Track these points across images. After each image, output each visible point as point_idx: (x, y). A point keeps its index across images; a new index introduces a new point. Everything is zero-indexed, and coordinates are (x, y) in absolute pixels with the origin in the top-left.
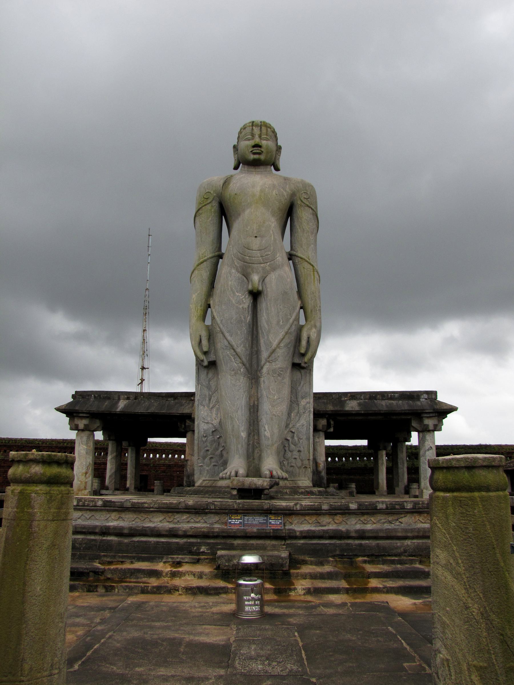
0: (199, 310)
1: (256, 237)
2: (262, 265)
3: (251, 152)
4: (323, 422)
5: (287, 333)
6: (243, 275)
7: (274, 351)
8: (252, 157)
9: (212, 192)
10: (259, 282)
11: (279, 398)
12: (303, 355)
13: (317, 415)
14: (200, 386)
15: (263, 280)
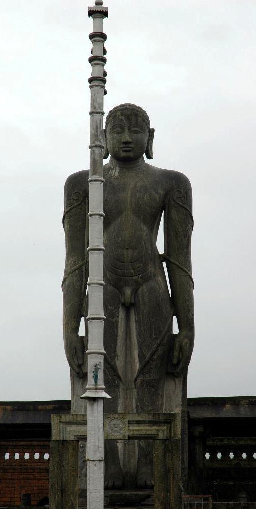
0: (73, 322)
1: (127, 249)
2: (134, 278)
3: (121, 148)
4: (199, 430)
5: (159, 345)
6: (115, 287)
7: (147, 362)
8: (123, 154)
9: (81, 193)
10: (132, 294)
11: (153, 410)
12: (178, 364)
13: (192, 423)
14: (75, 396)
15: (135, 292)
